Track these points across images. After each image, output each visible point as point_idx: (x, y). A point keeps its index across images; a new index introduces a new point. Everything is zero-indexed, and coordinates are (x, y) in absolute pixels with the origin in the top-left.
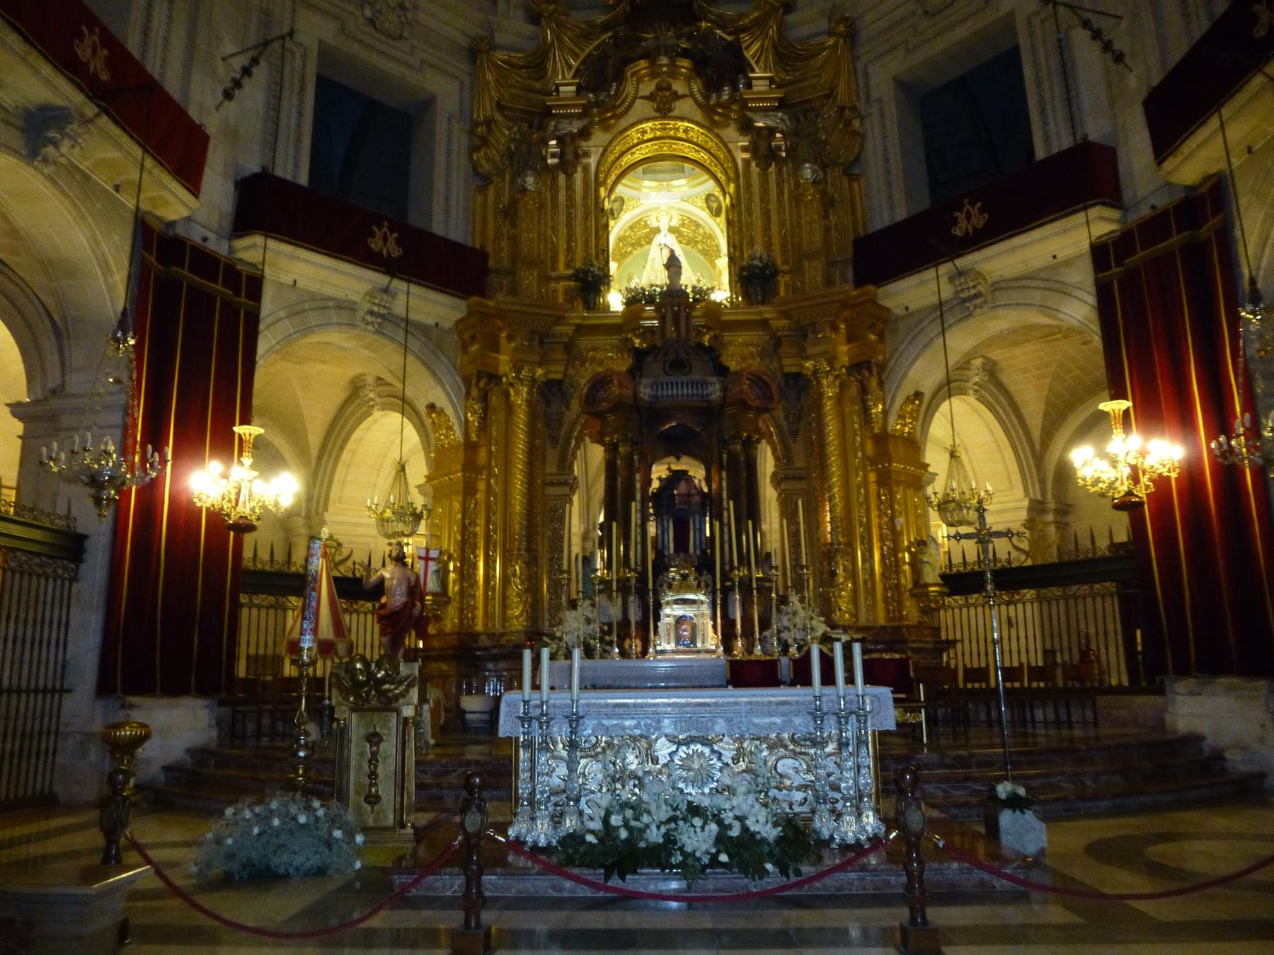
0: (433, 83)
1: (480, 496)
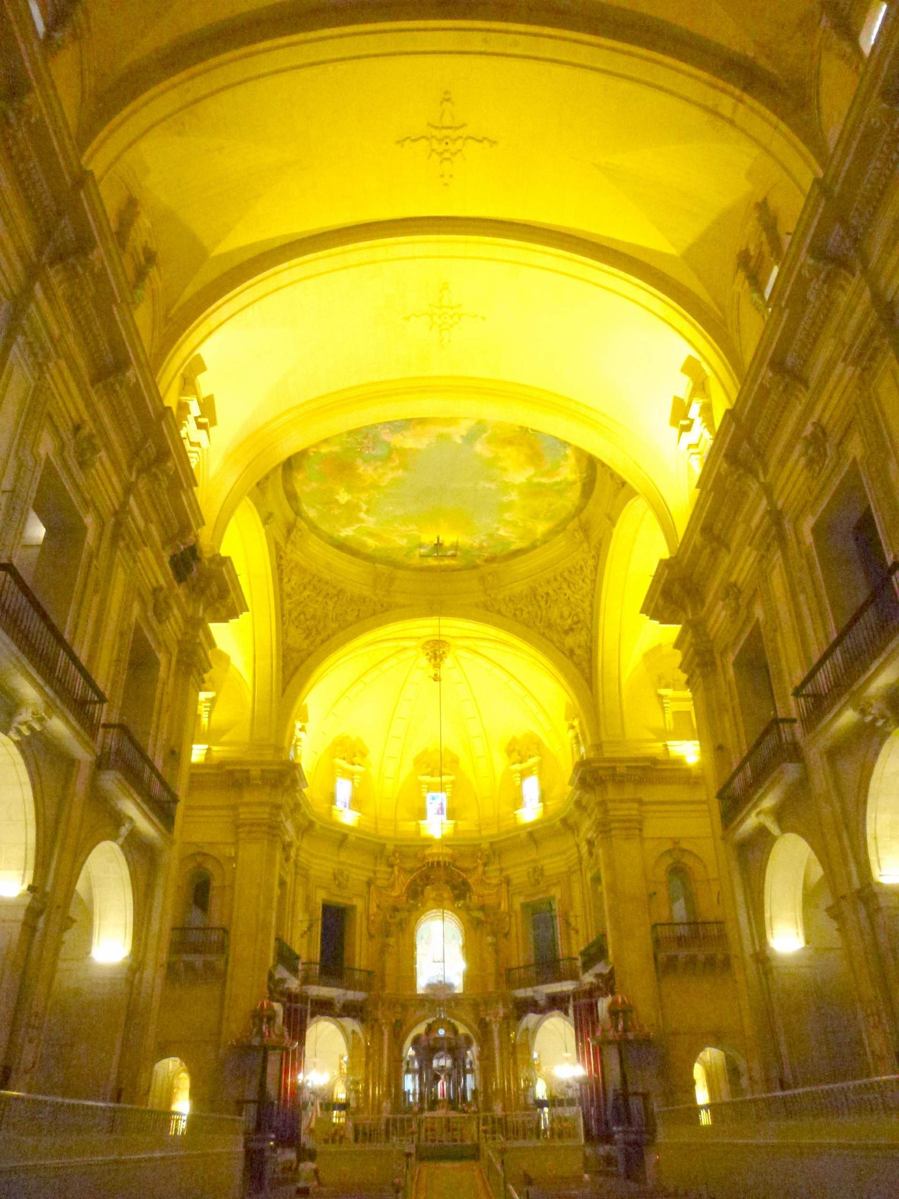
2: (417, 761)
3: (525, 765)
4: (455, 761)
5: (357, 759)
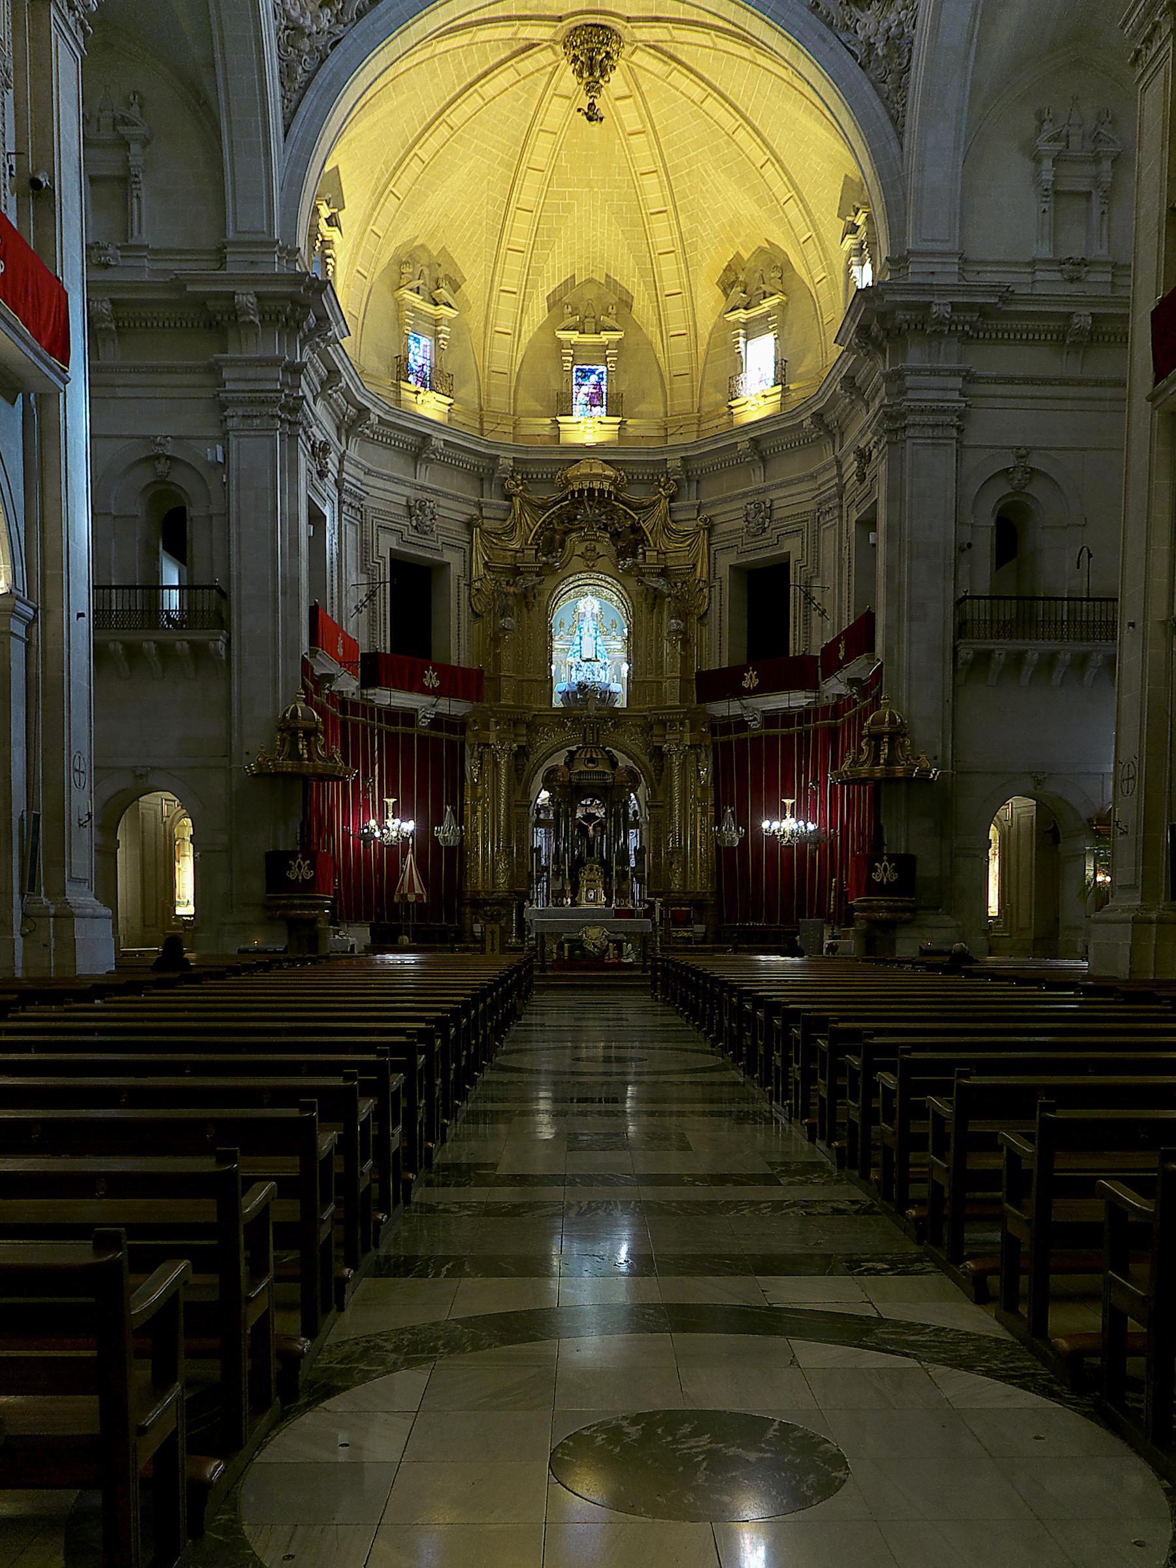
0: (449, 556)
1: (479, 814)
2: (555, 302)
3: (755, 312)
4: (626, 302)
5: (444, 293)
